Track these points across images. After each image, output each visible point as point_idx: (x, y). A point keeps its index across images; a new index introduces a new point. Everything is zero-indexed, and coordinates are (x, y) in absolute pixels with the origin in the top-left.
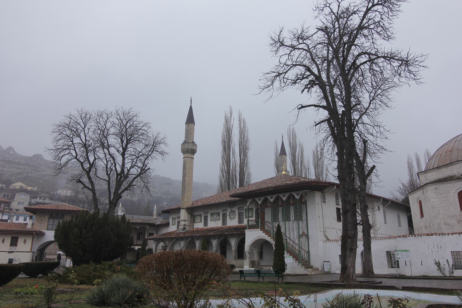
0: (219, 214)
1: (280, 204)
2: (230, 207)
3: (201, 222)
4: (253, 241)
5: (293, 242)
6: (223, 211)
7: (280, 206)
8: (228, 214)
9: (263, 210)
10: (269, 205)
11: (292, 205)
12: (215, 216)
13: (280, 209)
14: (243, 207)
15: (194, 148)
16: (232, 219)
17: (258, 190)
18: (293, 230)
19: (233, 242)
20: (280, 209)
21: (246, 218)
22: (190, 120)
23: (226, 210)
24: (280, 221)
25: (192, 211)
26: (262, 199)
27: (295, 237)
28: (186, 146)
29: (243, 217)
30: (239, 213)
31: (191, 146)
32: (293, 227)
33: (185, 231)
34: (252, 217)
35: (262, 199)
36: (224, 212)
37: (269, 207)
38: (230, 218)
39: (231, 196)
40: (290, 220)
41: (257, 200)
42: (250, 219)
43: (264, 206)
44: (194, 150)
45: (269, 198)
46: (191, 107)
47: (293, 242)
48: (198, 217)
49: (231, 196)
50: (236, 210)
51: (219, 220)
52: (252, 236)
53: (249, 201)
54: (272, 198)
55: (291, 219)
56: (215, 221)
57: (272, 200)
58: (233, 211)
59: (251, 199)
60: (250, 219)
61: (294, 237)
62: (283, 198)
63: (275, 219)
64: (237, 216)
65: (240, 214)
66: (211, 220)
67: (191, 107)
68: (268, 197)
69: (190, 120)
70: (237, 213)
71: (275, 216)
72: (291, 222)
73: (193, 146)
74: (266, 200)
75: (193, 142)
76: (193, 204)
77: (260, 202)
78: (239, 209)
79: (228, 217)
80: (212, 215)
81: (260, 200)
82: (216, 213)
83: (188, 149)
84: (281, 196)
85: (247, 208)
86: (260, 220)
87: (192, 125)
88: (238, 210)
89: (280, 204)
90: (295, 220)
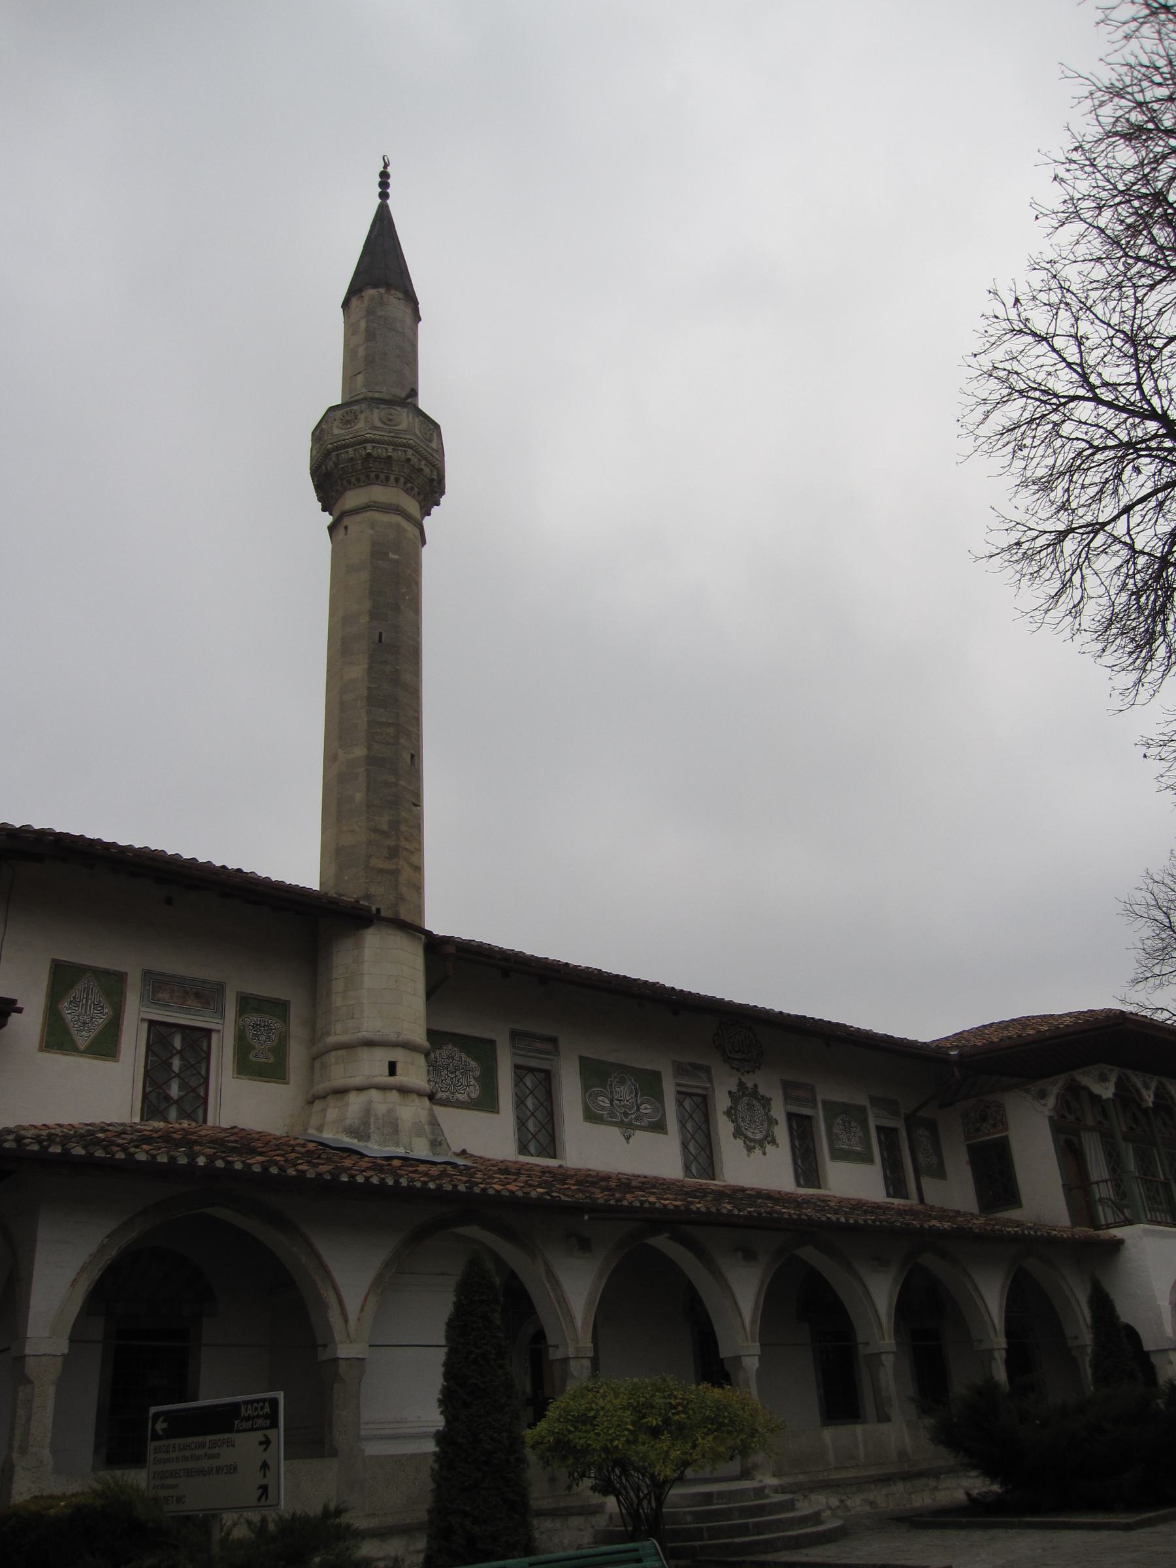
0: (650, 1083)
8: (722, 1102)
12: (624, 1093)
23: (707, 1070)
30: (790, 1116)
38: (738, 1133)
51: (659, 1127)
56: (628, 1127)
58: (754, 1093)
64: (781, 1132)
65: (801, 1129)
70: (778, 1111)
78: (788, 1087)
79: (724, 1128)
80: (595, 1074)
88: (787, 1099)
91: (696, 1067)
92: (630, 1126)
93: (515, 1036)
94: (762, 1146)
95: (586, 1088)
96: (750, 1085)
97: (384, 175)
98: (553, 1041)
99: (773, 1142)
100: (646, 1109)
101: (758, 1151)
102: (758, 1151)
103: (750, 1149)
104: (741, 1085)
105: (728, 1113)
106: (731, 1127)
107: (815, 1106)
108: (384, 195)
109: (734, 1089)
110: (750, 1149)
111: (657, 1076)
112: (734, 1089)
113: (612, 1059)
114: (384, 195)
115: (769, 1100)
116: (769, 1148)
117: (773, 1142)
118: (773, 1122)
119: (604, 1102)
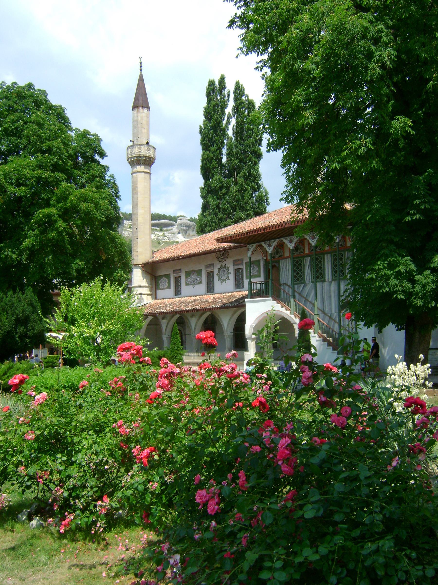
0: (199, 272)
1: (307, 251)
2: (219, 260)
3: (169, 287)
4: (261, 318)
5: (330, 318)
6: (207, 267)
7: (307, 256)
8: (216, 272)
9: (277, 264)
10: (287, 254)
11: (327, 253)
12: (193, 277)
13: (308, 261)
14: (242, 260)
15: (151, 153)
16: (222, 281)
17: (265, 228)
18: (330, 297)
19: (227, 322)
20: (308, 261)
21: (247, 278)
22: (141, 101)
23: (213, 265)
24: (307, 282)
25: (152, 270)
26: (274, 243)
27: (333, 311)
28: (136, 152)
29: (242, 278)
31: (144, 152)
32: (330, 291)
33: (142, 304)
34: (259, 276)
35: (274, 243)
36: (209, 270)
37: (288, 257)
38: (219, 279)
39: (218, 240)
40: (324, 281)
41: (265, 246)
42: (253, 280)
43: (277, 256)
44: (149, 158)
45: (286, 241)
46: (141, 76)
47: (330, 318)
48: (163, 279)
49: (218, 240)
50: (229, 263)
51: (201, 283)
52: (257, 311)
53: (252, 247)
54: (291, 242)
55: (327, 278)
56: (194, 284)
57: (291, 246)
58: (225, 267)
59: (255, 245)
60: (253, 280)
61: (331, 309)
62: (311, 241)
63: (298, 279)
64: (232, 276)
65: (238, 272)
66: (187, 284)
67: (141, 76)
68: (284, 241)
69: (141, 101)
70: (231, 270)
71: (298, 273)
72: (326, 285)
73: (149, 150)
74: (281, 246)
75: (148, 143)
76: (153, 257)
77: (270, 250)
78: (235, 263)
79: (216, 278)
81: (270, 246)
82: (195, 271)
83: (140, 157)
84: (308, 238)
85: (248, 260)
86: (270, 281)
87: (145, 110)
88: (234, 265)
89: (307, 251)
90: (333, 280)
91: (210, 265)
92: (195, 284)
93: (174, 271)
94: (225, 280)
95: (186, 278)
96: (224, 265)
97: (141, 63)
98: (180, 270)
99: (229, 279)
100: (198, 279)
101: (224, 282)
102: (224, 282)
103: (222, 282)
104: (222, 266)
105: (217, 275)
106: (218, 278)
107: (242, 264)
108: (141, 70)
109: (219, 267)
110: (222, 282)
111: (201, 270)
112: (219, 267)
113: (192, 269)
114: (141, 70)
115: (228, 268)
116: (227, 281)
117: (229, 279)
118: (229, 273)
119: (189, 280)
